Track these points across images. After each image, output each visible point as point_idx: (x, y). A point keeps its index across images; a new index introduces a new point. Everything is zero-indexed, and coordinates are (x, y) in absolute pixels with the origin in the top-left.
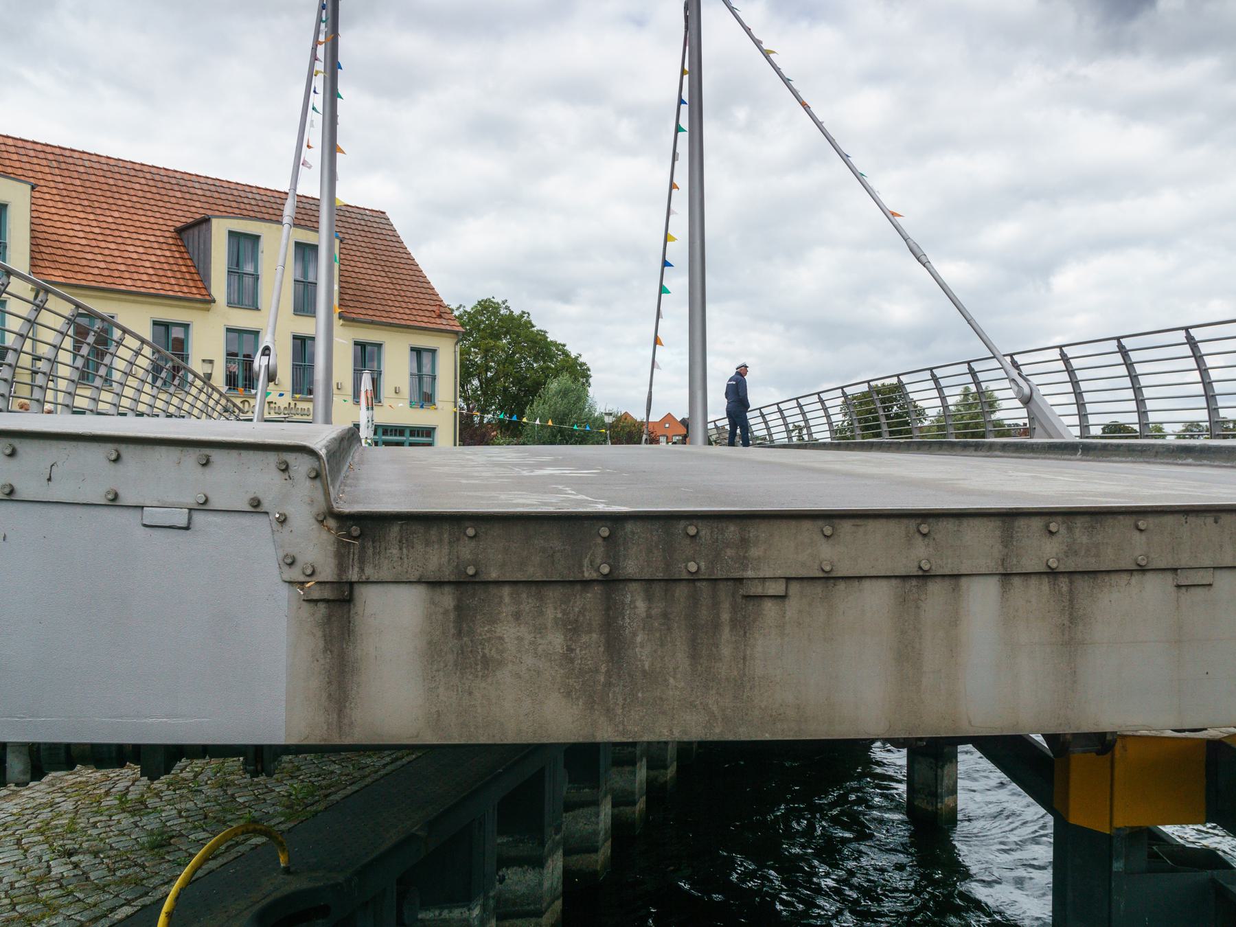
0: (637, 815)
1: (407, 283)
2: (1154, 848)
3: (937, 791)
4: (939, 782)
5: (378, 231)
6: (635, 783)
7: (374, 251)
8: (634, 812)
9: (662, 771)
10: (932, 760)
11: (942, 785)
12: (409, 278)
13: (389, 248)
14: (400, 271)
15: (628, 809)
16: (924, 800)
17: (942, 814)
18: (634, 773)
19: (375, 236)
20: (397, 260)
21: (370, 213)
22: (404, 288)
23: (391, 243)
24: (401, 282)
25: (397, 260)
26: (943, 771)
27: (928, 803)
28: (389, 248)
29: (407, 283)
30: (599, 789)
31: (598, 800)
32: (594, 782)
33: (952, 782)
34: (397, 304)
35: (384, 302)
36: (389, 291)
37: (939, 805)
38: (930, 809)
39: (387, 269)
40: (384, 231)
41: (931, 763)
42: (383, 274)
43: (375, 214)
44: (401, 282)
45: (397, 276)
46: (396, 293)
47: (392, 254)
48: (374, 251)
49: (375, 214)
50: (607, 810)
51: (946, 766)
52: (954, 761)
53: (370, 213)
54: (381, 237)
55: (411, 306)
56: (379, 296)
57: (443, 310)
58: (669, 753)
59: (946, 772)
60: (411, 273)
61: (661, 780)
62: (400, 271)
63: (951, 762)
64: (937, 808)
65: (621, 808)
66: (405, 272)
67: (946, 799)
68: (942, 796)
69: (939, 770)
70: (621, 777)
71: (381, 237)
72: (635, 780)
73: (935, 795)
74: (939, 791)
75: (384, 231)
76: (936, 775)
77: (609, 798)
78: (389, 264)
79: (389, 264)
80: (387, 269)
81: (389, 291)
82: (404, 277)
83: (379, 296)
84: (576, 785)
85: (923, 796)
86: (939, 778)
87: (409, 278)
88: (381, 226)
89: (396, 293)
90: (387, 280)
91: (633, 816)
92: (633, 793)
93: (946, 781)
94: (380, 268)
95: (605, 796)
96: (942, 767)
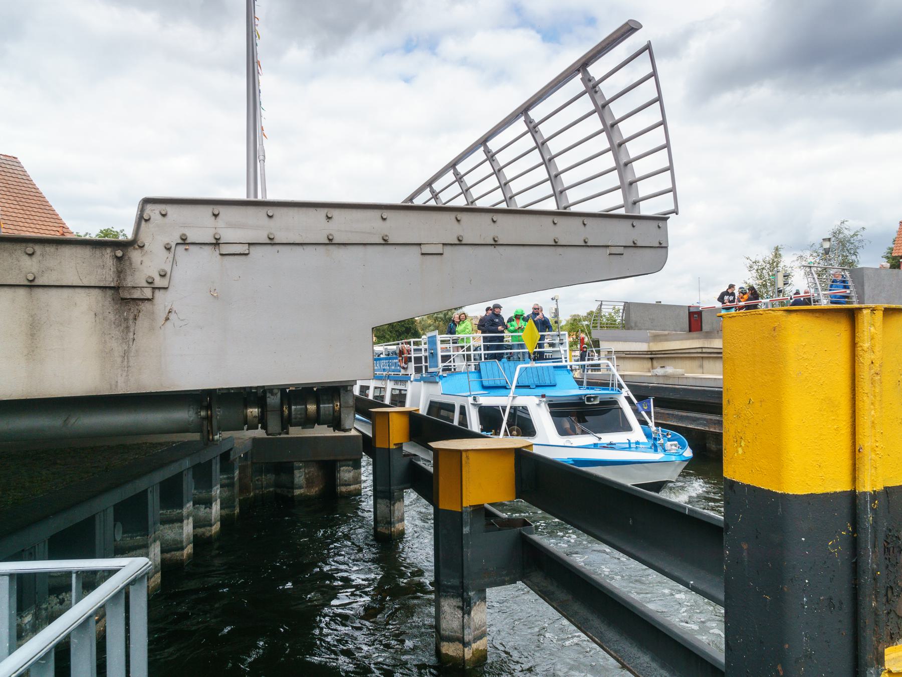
0: (185, 557)
1: (36, 210)
2: (492, 520)
3: (391, 520)
4: (392, 514)
5: (11, 171)
6: (183, 535)
7: (7, 186)
8: (182, 555)
9: (208, 528)
10: (387, 500)
11: (393, 515)
12: (37, 206)
13: (20, 184)
14: (29, 201)
15: (178, 553)
16: (383, 527)
17: (394, 535)
18: (182, 528)
19: (9, 174)
20: (27, 193)
21: (4, 158)
22: (33, 213)
23: (22, 181)
24: (30, 209)
25: (27, 193)
26: (394, 507)
27: (386, 528)
28: (20, 184)
29: (36, 210)
30: (148, 535)
31: (148, 544)
32: (144, 530)
33: (400, 514)
34: (26, 225)
35: (15, 223)
36: (21, 216)
37: (393, 529)
38: (387, 532)
39: (18, 199)
40: (16, 172)
41: (386, 503)
42: (15, 203)
43: (8, 158)
44: (30, 209)
45: (27, 205)
46: (26, 217)
47: (23, 188)
48: (7, 186)
49: (8, 158)
50: (156, 551)
51: (396, 504)
52: (401, 500)
53: (4, 158)
54: (13, 175)
55: (38, 227)
56: (12, 218)
57: (65, 230)
58: (213, 515)
59: (396, 507)
60: (39, 203)
61: (208, 534)
62: (29, 201)
63: (400, 501)
64: (391, 531)
65: (173, 553)
66: (34, 202)
67: (397, 525)
68: (394, 523)
69: (392, 507)
70: (172, 531)
71: (13, 175)
72: (183, 532)
73: (390, 523)
74: (392, 520)
75: (16, 172)
76: (390, 510)
77: (158, 543)
78: (20, 196)
79: (20, 196)
80: (18, 199)
81: (21, 216)
82: (32, 205)
83: (12, 218)
84: (130, 535)
85: (383, 525)
86: (392, 512)
87: (37, 206)
88: (13, 167)
89: (26, 217)
90: (18, 207)
91: (182, 558)
92: (182, 542)
93: (397, 514)
94: (12, 198)
95: (155, 541)
96: (394, 504)
